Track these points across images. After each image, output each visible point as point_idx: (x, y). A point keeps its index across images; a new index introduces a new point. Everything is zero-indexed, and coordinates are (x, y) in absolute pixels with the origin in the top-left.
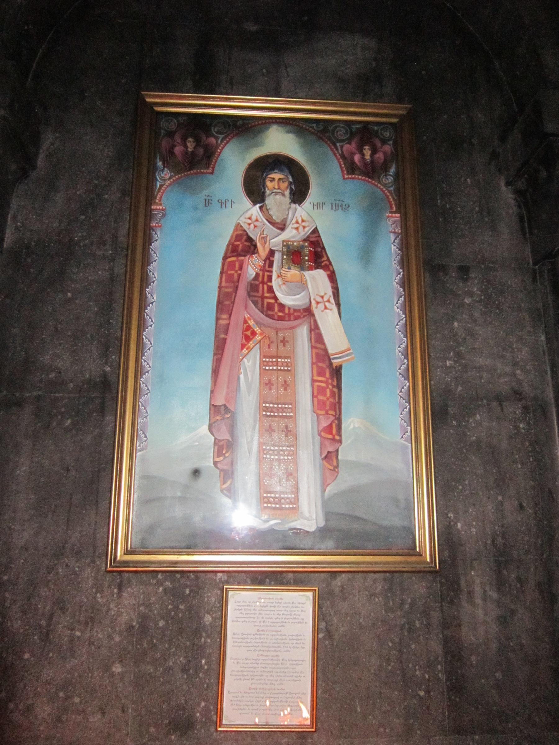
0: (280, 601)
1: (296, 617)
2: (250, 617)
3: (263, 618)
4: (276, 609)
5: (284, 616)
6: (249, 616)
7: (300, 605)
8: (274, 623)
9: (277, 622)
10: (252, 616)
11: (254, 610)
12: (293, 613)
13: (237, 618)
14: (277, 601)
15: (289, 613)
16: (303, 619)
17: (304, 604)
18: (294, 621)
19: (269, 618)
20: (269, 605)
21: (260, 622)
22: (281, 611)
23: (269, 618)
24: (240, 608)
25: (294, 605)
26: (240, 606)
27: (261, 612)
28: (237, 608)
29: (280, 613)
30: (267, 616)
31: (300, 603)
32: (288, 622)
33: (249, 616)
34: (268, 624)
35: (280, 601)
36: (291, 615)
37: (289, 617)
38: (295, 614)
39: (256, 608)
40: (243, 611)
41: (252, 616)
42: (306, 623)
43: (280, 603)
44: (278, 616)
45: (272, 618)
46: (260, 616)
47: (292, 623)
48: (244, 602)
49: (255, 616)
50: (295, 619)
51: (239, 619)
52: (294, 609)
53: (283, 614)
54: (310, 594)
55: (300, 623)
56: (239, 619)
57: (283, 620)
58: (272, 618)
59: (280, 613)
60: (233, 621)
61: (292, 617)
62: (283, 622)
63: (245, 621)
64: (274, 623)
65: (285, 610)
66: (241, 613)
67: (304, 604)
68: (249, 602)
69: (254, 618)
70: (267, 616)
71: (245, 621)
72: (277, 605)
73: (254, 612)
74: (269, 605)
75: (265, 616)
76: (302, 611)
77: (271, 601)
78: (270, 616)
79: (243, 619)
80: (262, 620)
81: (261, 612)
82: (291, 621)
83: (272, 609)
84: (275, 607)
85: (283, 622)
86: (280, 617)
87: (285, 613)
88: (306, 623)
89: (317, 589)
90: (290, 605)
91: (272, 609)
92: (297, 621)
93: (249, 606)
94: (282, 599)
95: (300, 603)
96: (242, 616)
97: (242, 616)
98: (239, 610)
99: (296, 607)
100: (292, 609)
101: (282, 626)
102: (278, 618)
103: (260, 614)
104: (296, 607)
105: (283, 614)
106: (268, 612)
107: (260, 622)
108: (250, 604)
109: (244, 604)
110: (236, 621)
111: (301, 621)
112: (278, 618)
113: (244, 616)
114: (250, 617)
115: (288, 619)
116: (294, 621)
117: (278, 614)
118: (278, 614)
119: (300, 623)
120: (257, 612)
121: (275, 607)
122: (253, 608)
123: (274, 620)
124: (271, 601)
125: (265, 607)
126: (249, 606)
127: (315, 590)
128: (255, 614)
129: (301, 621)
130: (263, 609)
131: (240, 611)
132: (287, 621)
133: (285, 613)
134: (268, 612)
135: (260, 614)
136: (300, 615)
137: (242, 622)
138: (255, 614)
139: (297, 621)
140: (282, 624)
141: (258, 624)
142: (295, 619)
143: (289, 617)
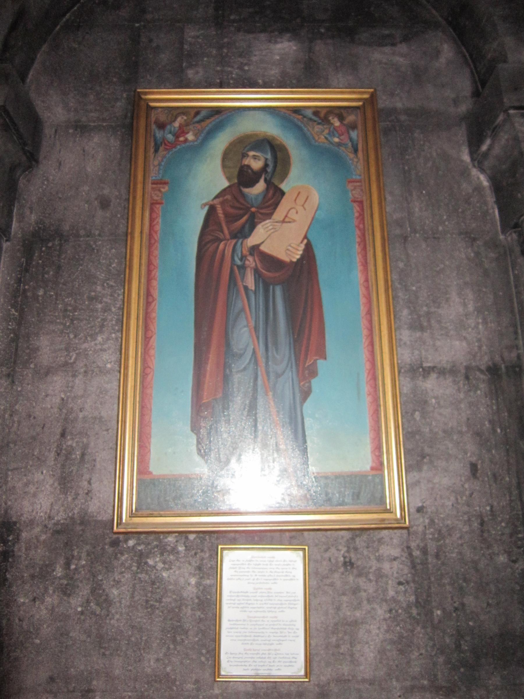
1: (288, 574)
5: (276, 574)
10: (246, 574)
11: (248, 568)
12: (285, 570)
16: (294, 576)
17: (295, 561)
21: (254, 580)
24: (235, 566)
25: (285, 563)
26: (234, 565)
27: (255, 570)
28: (232, 566)
30: (260, 574)
35: (272, 559)
37: (281, 574)
41: (246, 574)
43: (273, 561)
45: (264, 576)
48: (238, 560)
50: (287, 576)
51: (233, 577)
52: (286, 567)
53: (275, 572)
54: (301, 553)
56: (233, 577)
58: (264, 576)
59: (272, 570)
60: (228, 579)
61: (284, 574)
62: (275, 579)
63: (239, 579)
65: (277, 568)
70: (260, 574)
71: (239, 579)
73: (247, 570)
76: (293, 568)
79: (238, 577)
80: (256, 578)
81: (255, 570)
83: (265, 567)
85: (275, 579)
86: (272, 574)
87: (278, 570)
91: (265, 567)
93: (243, 564)
95: (291, 561)
96: (236, 574)
97: (236, 574)
98: (234, 568)
99: (288, 565)
101: (275, 583)
102: (270, 575)
103: (253, 572)
104: (288, 565)
105: (275, 572)
106: (261, 570)
107: (254, 580)
109: (237, 563)
110: (231, 579)
112: (270, 575)
117: (271, 572)
118: (271, 572)
119: (291, 579)
123: (266, 578)
126: (243, 564)
128: (248, 572)
130: (256, 567)
134: (261, 570)
135: (253, 572)
138: (248, 572)
143: (281, 574)
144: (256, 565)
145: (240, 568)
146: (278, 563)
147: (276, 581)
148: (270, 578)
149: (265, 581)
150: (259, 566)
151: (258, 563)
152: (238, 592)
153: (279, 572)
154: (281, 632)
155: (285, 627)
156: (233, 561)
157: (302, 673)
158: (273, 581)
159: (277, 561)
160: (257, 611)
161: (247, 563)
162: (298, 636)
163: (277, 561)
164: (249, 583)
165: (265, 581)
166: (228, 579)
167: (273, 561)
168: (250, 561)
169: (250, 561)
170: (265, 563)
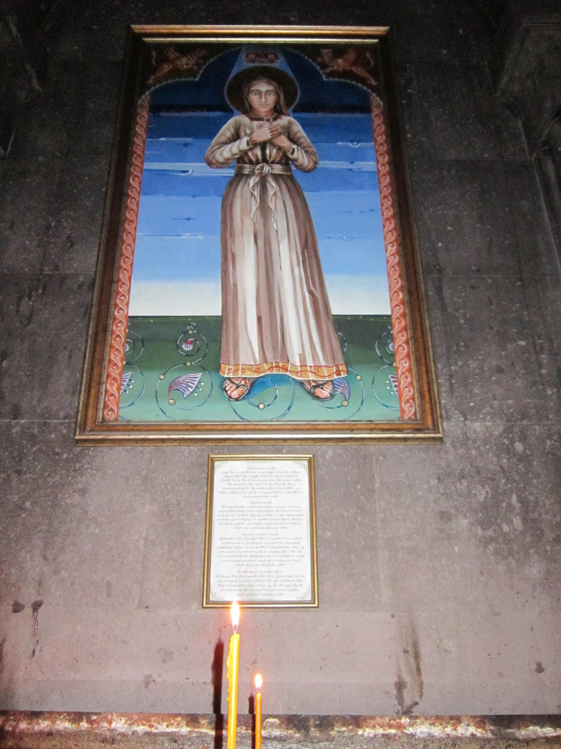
1: (290, 486)
2: (239, 488)
4: (268, 478)
5: (277, 486)
7: (295, 474)
8: (266, 493)
9: (270, 493)
10: (241, 486)
11: (243, 480)
12: (287, 483)
13: (224, 489)
14: (268, 471)
15: (283, 483)
16: (298, 489)
17: (299, 472)
19: (261, 488)
20: (259, 474)
21: (250, 493)
22: (274, 480)
23: (261, 488)
25: (287, 474)
26: (228, 477)
28: (225, 478)
30: (258, 486)
31: (294, 472)
32: (282, 492)
35: (272, 471)
36: (284, 484)
38: (289, 484)
39: (245, 478)
40: (230, 482)
41: (241, 486)
42: (302, 492)
43: (272, 473)
44: (271, 486)
45: (263, 488)
46: (249, 486)
47: (286, 493)
48: (232, 472)
49: (245, 486)
50: (289, 488)
51: (226, 491)
53: (276, 484)
55: (295, 492)
56: (226, 491)
58: (263, 488)
59: (272, 482)
60: (220, 492)
61: (287, 486)
62: (276, 492)
63: (233, 492)
64: (266, 493)
65: (278, 480)
66: (229, 484)
67: (299, 472)
68: (238, 473)
69: (244, 489)
70: (258, 486)
71: (233, 492)
74: (259, 474)
76: (297, 480)
77: (262, 470)
78: (261, 486)
83: (263, 478)
84: (266, 476)
85: (276, 492)
86: (273, 487)
88: (302, 492)
90: (284, 474)
91: (263, 478)
92: (291, 490)
93: (238, 476)
94: (274, 468)
95: (294, 472)
96: (229, 486)
97: (229, 486)
98: (227, 481)
99: (289, 476)
100: (286, 478)
101: (275, 496)
102: (270, 488)
103: (250, 484)
104: (289, 476)
105: (276, 484)
107: (250, 493)
108: (239, 474)
110: (224, 493)
111: (297, 490)
112: (270, 488)
113: (233, 487)
114: (239, 488)
115: (281, 488)
116: (288, 490)
117: (270, 484)
118: (270, 484)
119: (295, 492)
120: (247, 482)
121: (266, 476)
122: (242, 478)
123: (265, 490)
124: (262, 470)
125: (256, 477)
128: (244, 484)
130: (254, 479)
131: (228, 482)
136: (294, 485)
137: (231, 493)
138: (244, 484)
140: (275, 494)
141: (247, 495)
142: (289, 488)
143: (282, 486)
144: (253, 476)
145: (234, 480)
146: (279, 474)
147: (277, 494)
148: (269, 490)
149: (264, 495)
150: (256, 479)
151: (255, 475)
152: (232, 507)
153: (279, 485)
154: (283, 552)
155: (287, 545)
156: (226, 473)
159: (278, 472)
160: (254, 528)
161: (242, 475)
162: (303, 556)
163: (278, 472)
164: (244, 497)
165: (264, 495)
167: (272, 473)
168: (246, 473)
169: (246, 473)
170: (263, 475)
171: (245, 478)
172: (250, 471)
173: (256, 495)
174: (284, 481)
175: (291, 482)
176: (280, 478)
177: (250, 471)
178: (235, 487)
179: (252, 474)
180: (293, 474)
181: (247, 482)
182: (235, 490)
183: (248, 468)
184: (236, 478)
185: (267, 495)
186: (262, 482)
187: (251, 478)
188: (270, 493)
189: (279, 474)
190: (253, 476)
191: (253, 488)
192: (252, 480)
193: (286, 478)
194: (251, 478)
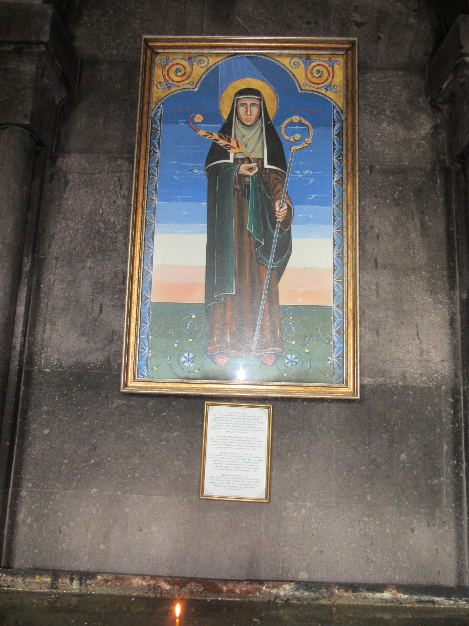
0: (245, 415)
3: (232, 426)
5: (247, 426)
6: (223, 425)
7: (260, 418)
9: (243, 430)
10: (225, 425)
12: (254, 424)
14: (243, 415)
15: (251, 423)
17: (262, 417)
18: (254, 429)
20: (237, 417)
21: (230, 429)
24: (217, 419)
25: (255, 418)
28: (215, 419)
29: (244, 423)
30: (236, 425)
33: (223, 425)
34: (236, 431)
35: (245, 415)
36: (252, 425)
38: (255, 425)
39: (228, 420)
40: (218, 422)
41: (225, 425)
46: (231, 425)
49: (227, 425)
51: (215, 427)
52: (255, 421)
54: (267, 410)
55: (259, 430)
56: (215, 427)
57: (247, 428)
59: (244, 423)
60: (211, 428)
61: (253, 426)
62: (247, 430)
67: (262, 417)
70: (236, 425)
72: (242, 418)
74: (237, 417)
75: (234, 425)
76: (260, 422)
77: (238, 415)
78: (238, 425)
80: (232, 428)
82: (252, 429)
84: (241, 419)
85: (247, 430)
87: (249, 423)
89: (271, 406)
90: (252, 418)
92: (257, 429)
93: (223, 418)
94: (246, 414)
96: (217, 424)
97: (217, 424)
100: (253, 421)
101: (246, 432)
103: (230, 423)
106: (236, 423)
107: (230, 429)
111: (260, 429)
113: (219, 425)
119: (259, 430)
120: (228, 422)
121: (241, 419)
122: (226, 419)
123: (240, 428)
124: (238, 415)
127: (270, 407)
128: (227, 423)
129: (260, 429)
130: (233, 420)
132: (249, 428)
133: (249, 423)
134: (236, 423)
139: (257, 429)
141: (229, 430)
143: (251, 426)
144: (232, 418)
145: (220, 420)
146: (249, 418)
147: (247, 431)
148: (243, 428)
150: (235, 420)
151: (234, 417)
157: (264, 496)
158: (244, 431)
161: (226, 417)
166: (211, 428)
168: (228, 415)
169: (228, 415)
170: (240, 418)
171: (228, 420)
172: (230, 414)
173: (234, 431)
174: (252, 422)
175: (257, 424)
176: (250, 421)
177: (230, 414)
178: (221, 425)
179: (232, 417)
180: (258, 418)
181: (228, 422)
182: (221, 427)
183: (230, 413)
184: (222, 419)
185: (241, 431)
186: (239, 423)
187: (231, 420)
188: (243, 430)
189: (249, 418)
190: (232, 418)
191: (232, 426)
192: (232, 421)
193: (253, 421)
194: (231, 420)
